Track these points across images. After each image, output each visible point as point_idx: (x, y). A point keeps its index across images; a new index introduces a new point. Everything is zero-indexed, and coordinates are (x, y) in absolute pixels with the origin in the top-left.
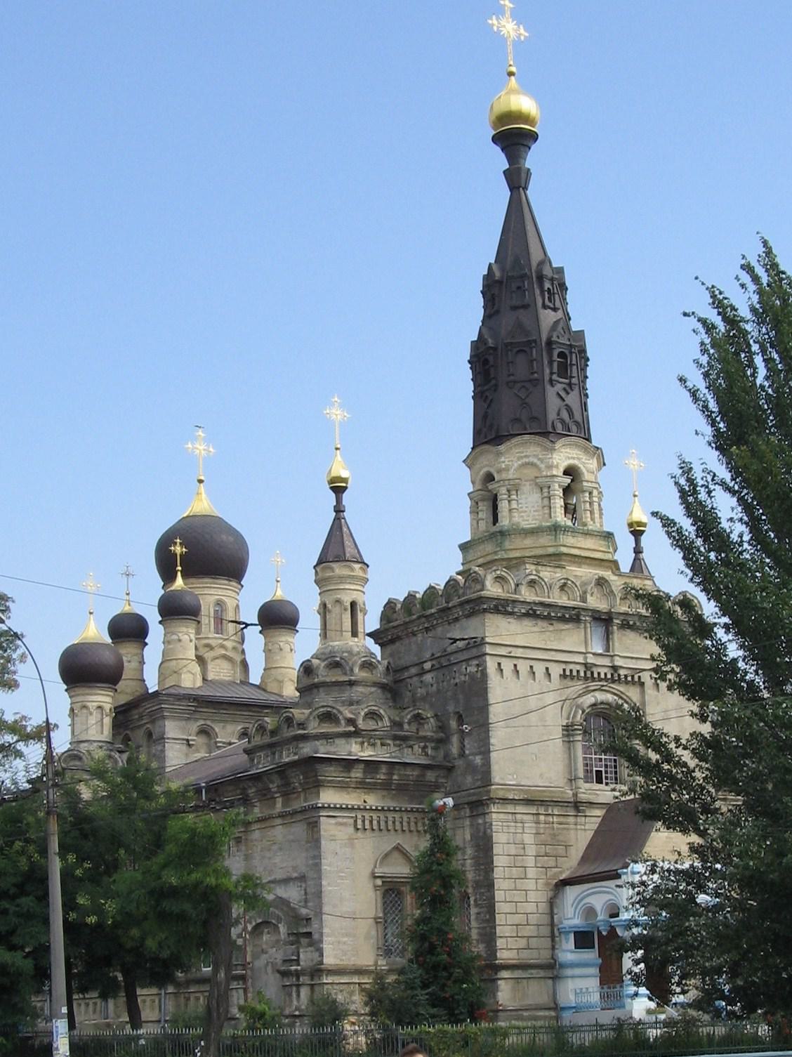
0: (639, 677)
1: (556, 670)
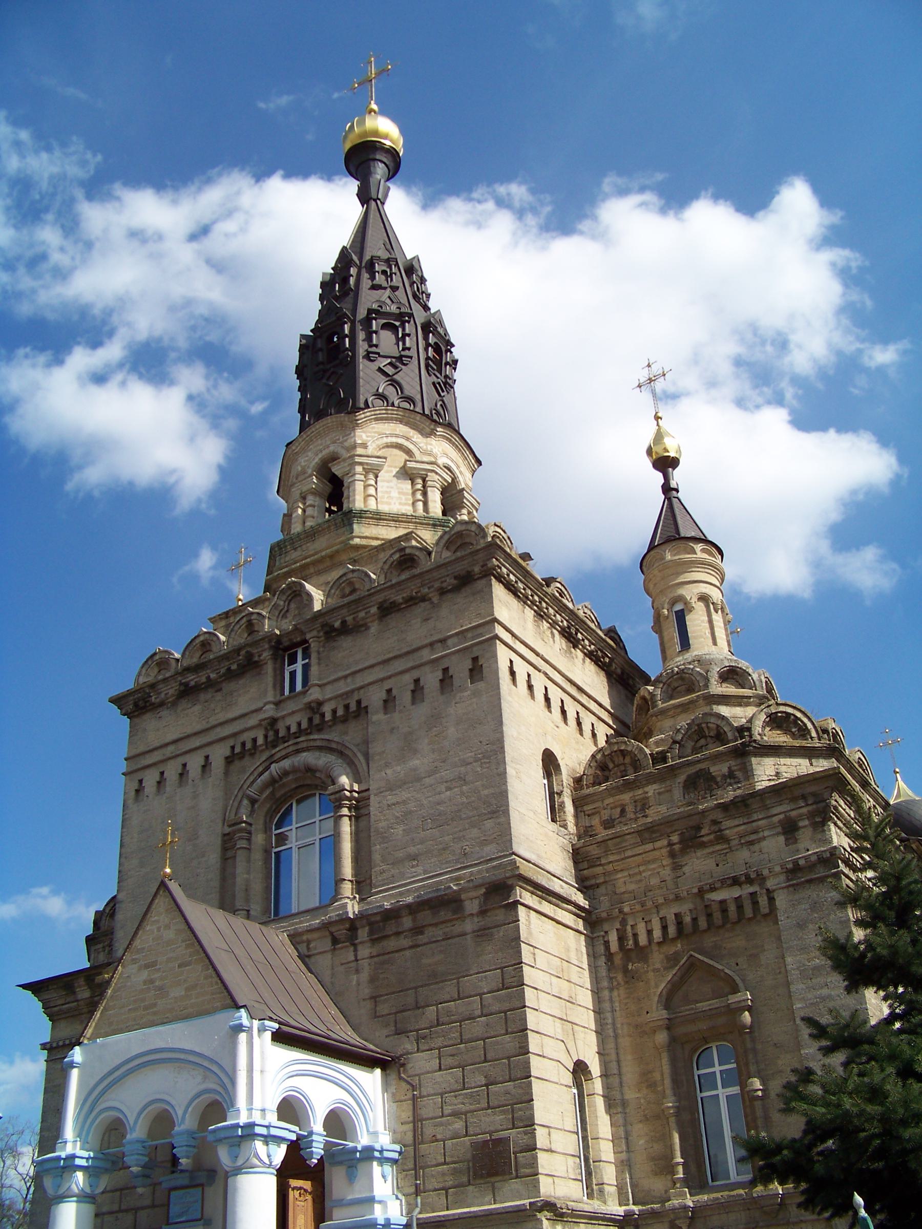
0: (359, 702)
1: (219, 754)
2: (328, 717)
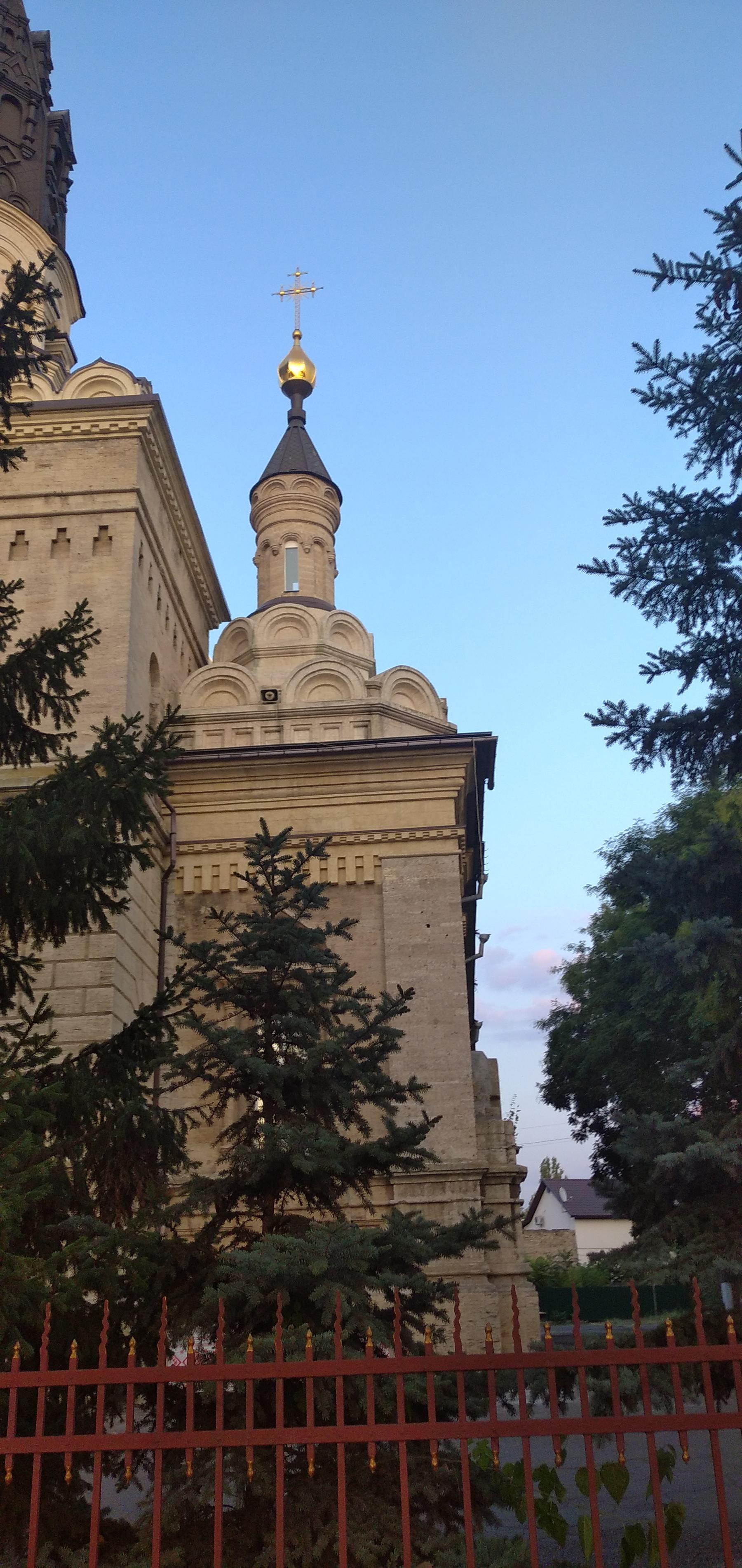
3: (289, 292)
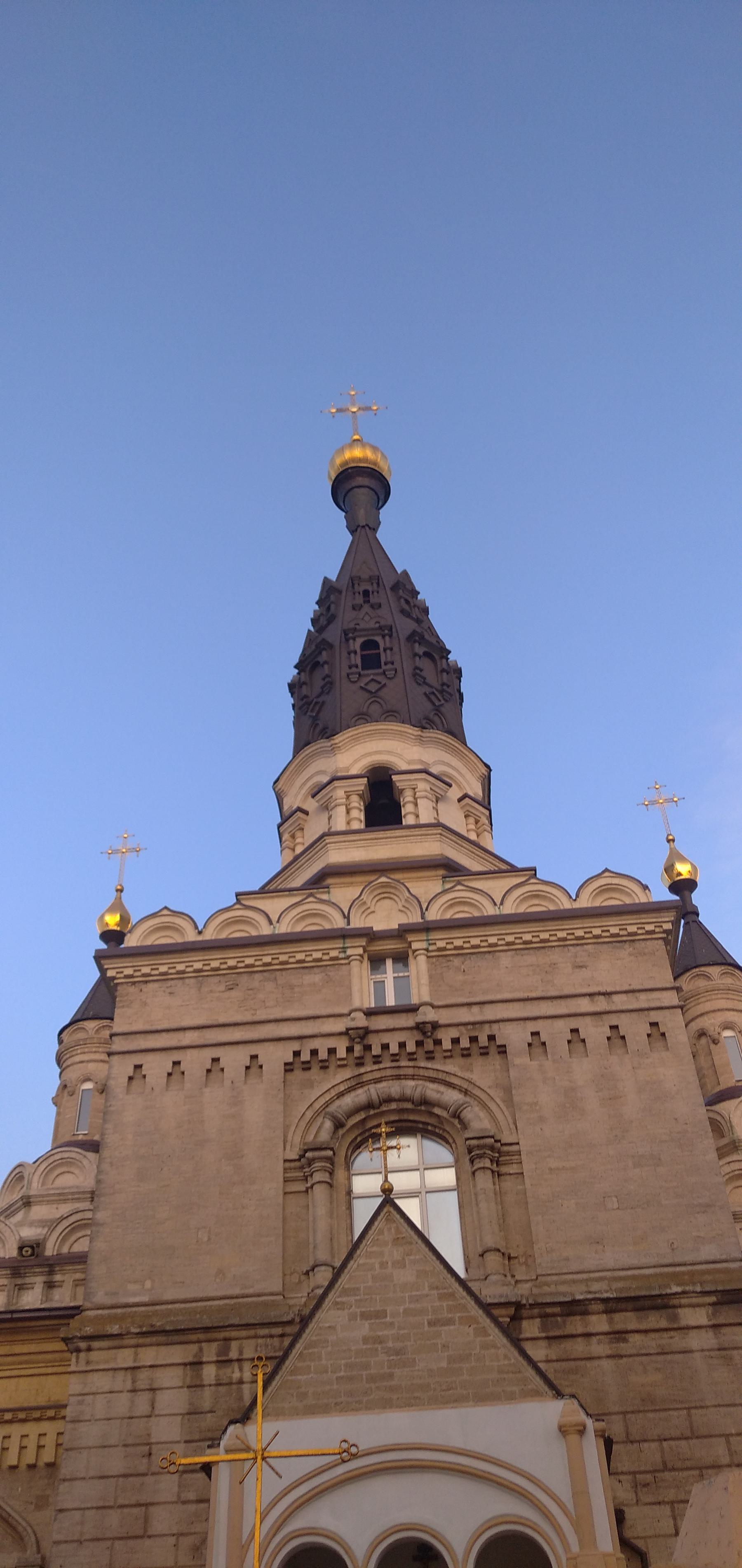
0: (492, 1038)
1: (275, 1057)
2: (447, 1045)
3: (653, 803)
